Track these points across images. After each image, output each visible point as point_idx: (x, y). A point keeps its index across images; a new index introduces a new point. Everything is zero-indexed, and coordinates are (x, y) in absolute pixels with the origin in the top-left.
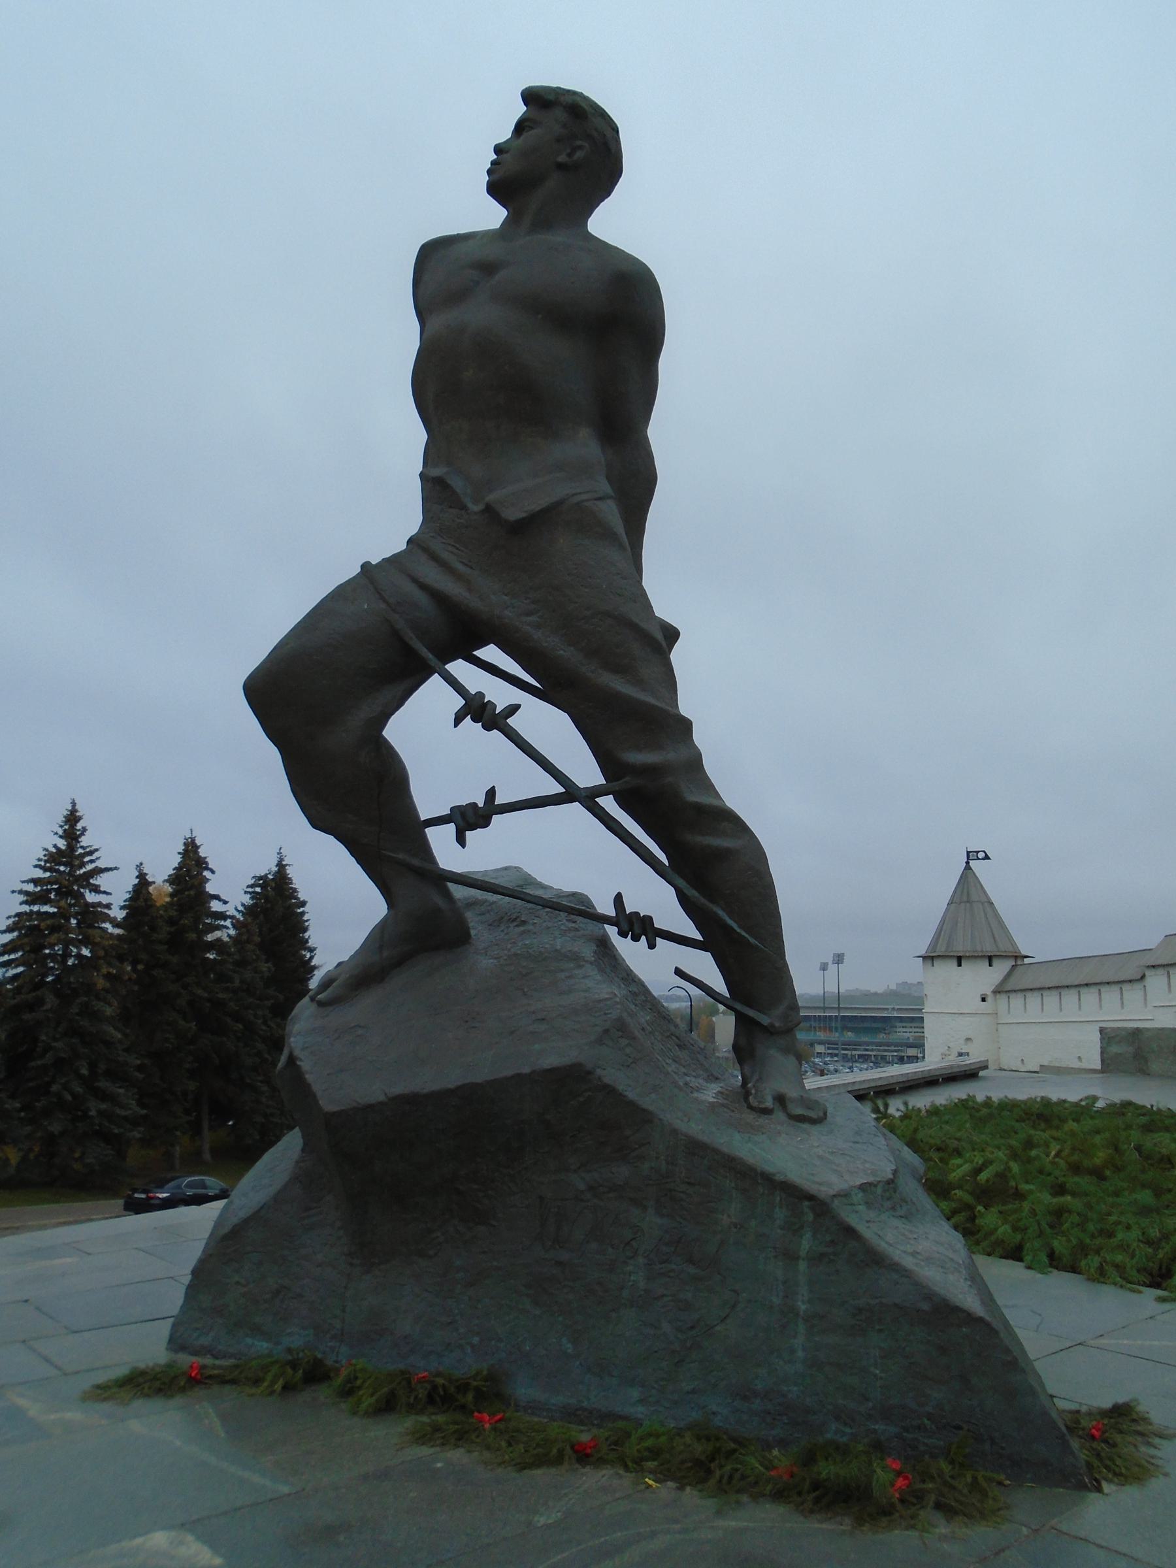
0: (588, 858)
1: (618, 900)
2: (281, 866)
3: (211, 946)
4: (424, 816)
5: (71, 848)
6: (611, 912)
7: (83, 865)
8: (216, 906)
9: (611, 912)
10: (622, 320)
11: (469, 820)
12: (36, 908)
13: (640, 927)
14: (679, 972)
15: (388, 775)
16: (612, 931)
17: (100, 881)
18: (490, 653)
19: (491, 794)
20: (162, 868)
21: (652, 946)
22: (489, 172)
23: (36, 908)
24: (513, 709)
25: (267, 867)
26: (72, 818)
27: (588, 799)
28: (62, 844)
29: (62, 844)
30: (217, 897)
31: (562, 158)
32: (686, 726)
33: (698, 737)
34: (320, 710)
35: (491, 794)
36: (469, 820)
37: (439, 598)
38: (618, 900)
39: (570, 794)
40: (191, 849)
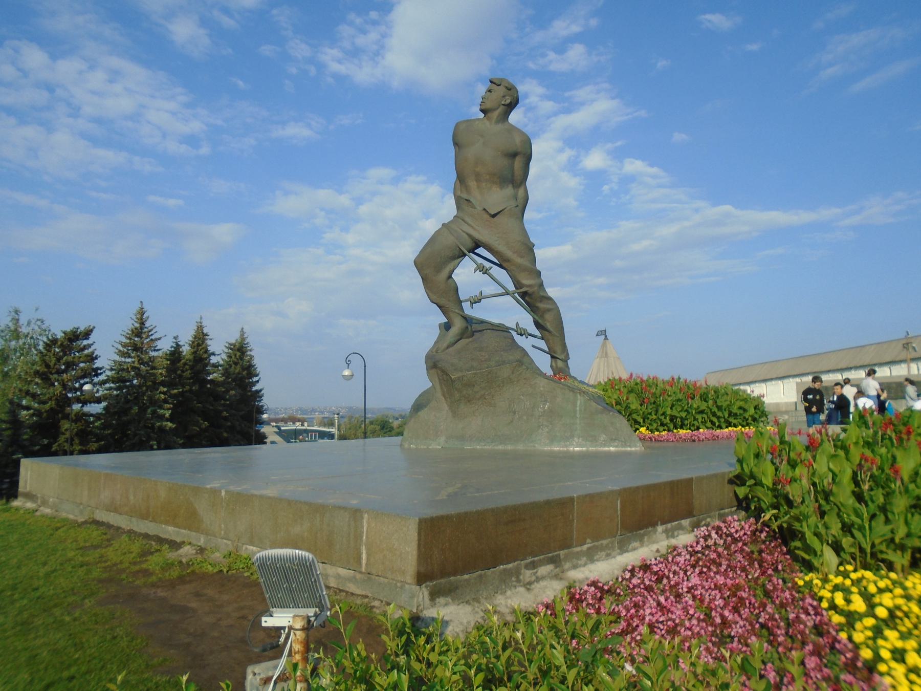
0: (509, 313)
1: (517, 324)
2: (243, 339)
3: (212, 381)
5: (141, 328)
7: (148, 336)
8: (214, 360)
11: (476, 301)
12: (123, 359)
14: (533, 346)
16: (514, 333)
17: (159, 345)
20: (186, 339)
23: (123, 359)
25: (234, 338)
26: (142, 312)
27: (512, 294)
28: (137, 325)
29: (137, 325)
30: (213, 354)
34: (435, 266)
36: (476, 301)
38: (517, 324)
39: (507, 293)
40: (200, 328)
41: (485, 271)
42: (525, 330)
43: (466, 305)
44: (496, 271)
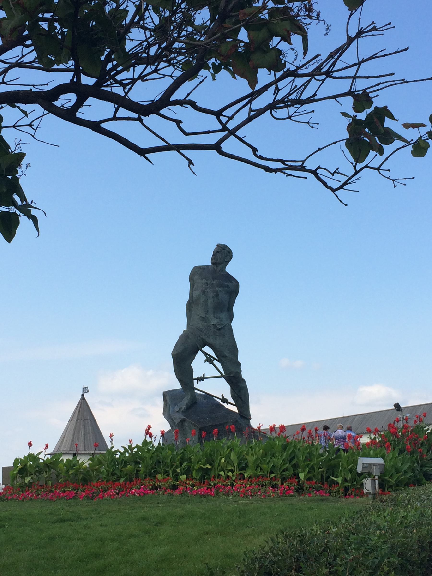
1: (222, 396)
4: (194, 378)
6: (221, 398)
9: (221, 398)
10: (231, 288)
13: (225, 400)
15: (192, 372)
16: (220, 401)
18: (207, 349)
19: (204, 375)
21: (227, 404)
22: (212, 260)
24: (214, 361)
31: (226, 260)
32: (239, 364)
33: (242, 368)
35: (204, 375)
37: (203, 339)
38: (222, 396)
39: (222, 376)
41: (211, 362)
42: (227, 400)
43: (195, 382)
44: (215, 362)
